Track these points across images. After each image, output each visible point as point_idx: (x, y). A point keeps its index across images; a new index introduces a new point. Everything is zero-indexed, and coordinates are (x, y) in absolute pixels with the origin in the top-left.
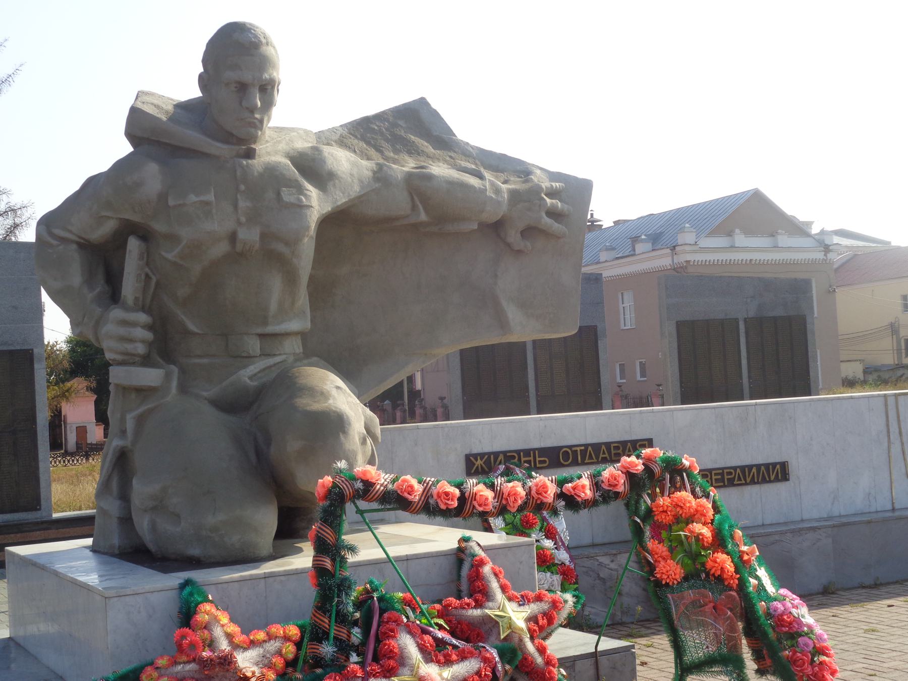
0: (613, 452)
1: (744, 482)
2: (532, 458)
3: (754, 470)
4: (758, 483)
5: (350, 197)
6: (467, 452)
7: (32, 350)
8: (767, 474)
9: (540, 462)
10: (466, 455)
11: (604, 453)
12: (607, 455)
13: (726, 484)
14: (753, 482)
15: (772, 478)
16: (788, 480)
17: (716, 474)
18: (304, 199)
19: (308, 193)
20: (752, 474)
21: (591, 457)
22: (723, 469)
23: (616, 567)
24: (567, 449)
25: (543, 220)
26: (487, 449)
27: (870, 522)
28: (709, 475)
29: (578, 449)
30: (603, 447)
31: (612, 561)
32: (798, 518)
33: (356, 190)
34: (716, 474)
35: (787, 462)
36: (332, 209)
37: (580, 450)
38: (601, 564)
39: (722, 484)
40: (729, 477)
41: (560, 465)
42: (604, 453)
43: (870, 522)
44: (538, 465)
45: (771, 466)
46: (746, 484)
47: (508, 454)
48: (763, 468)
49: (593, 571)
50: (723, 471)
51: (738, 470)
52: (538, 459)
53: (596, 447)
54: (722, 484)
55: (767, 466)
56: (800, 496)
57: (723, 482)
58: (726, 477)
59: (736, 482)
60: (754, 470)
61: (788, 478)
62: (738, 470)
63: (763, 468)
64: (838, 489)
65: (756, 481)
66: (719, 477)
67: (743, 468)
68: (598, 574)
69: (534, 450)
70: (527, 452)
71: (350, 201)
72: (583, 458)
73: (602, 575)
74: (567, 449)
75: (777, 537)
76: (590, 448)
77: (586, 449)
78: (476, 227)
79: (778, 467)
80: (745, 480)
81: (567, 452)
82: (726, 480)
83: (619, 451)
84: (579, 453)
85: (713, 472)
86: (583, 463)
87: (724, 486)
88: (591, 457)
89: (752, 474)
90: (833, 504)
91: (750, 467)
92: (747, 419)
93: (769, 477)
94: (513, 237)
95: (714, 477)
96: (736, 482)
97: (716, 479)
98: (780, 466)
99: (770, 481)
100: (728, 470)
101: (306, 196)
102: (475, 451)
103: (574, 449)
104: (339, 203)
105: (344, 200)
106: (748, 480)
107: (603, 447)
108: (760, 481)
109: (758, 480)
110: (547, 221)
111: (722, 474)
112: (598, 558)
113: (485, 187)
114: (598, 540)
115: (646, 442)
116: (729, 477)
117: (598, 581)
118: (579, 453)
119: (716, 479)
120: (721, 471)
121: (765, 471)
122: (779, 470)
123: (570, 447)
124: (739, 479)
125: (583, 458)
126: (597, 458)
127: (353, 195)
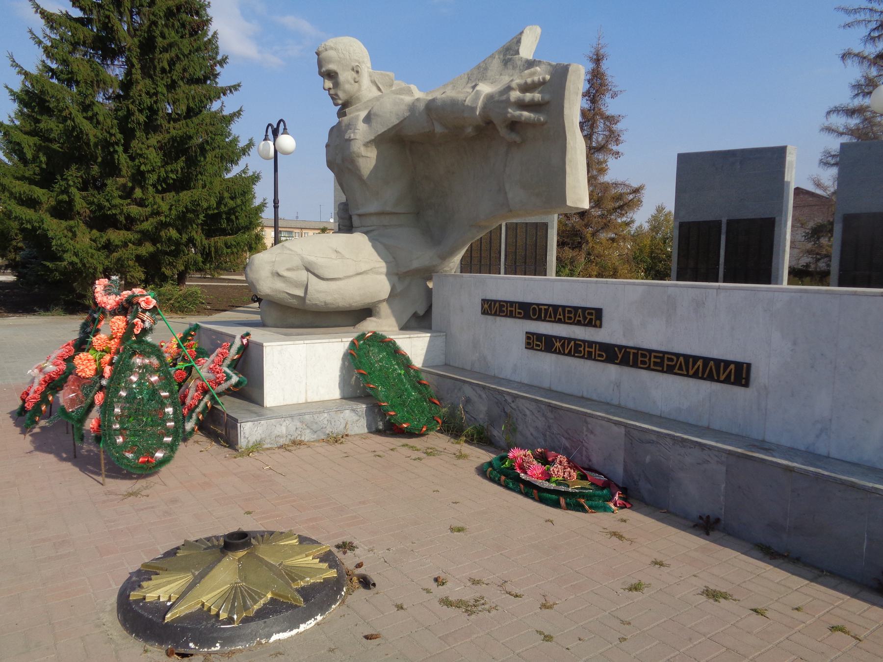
0: (567, 315)
1: (686, 373)
2: (514, 309)
3: (700, 363)
4: (702, 378)
5: (388, 128)
6: (484, 298)
7: (775, 218)
8: (716, 374)
9: (520, 313)
10: (482, 300)
11: (560, 315)
12: (562, 317)
13: (665, 370)
14: (695, 376)
15: (722, 378)
16: (746, 385)
17: (655, 357)
18: (352, 135)
19: (356, 131)
20: (696, 367)
21: (550, 317)
22: (664, 353)
23: (515, 407)
24: (536, 307)
25: (509, 115)
26: (494, 298)
27: (791, 471)
28: (648, 355)
29: (543, 307)
30: (560, 309)
31: (513, 402)
32: (760, 438)
33: (395, 121)
34: (655, 357)
35: (749, 365)
36: (376, 138)
37: (545, 309)
38: (506, 400)
39: (661, 369)
40: (670, 363)
41: (530, 318)
42: (560, 315)
43: (791, 471)
44: (517, 315)
45: (722, 364)
46: (687, 375)
47: (501, 303)
48: (712, 363)
49: (501, 404)
50: (664, 357)
51: (681, 359)
52: (517, 310)
53: (556, 307)
54: (661, 369)
55: (718, 362)
56: (766, 410)
57: (663, 366)
58: (666, 362)
59: (676, 371)
60: (700, 363)
61: (743, 381)
62: (681, 359)
63: (712, 363)
64: (830, 420)
65: (700, 375)
66: (659, 360)
67: (687, 357)
68: (504, 410)
69: (516, 303)
70: (512, 303)
71: (389, 130)
72: (545, 317)
73: (506, 410)
74: (536, 307)
75: (654, 438)
76: (551, 309)
77: (549, 308)
78: (469, 130)
79: (732, 366)
80: (687, 371)
81: (534, 309)
82: (665, 366)
83: (571, 315)
84: (543, 311)
85: (653, 354)
86: (545, 320)
87: (662, 371)
88: (550, 317)
89: (696, 367)
90: (818, 436)
91: (696, 358)
92: (704, 303)
93: (718, 376)
94: (503, 132)
95: (653, 359)
96: (675, 371)
97: (654, 362)
98: (735, 367)
99: (718, 381)
100: (670, 356)
101: (354, 133)
102: (488, 298)
103: (541, 307)
104: (379, 133)
105: (383, 131)
106: (691, 372)
107: (560, 309)
108: (705, 377)
109: (703, 373)
110: (513, 113)
111: (662, 359)
112: (504, 395)
113: (466, 98)
114: (554, 388)
115: (593, 311)
116: (670, 363)
117: (503, 413)
118: (543, 311)
119: (654, 362)
120: (661, 355)
121: (713, 367)
122: (733, 371)
123: (538, 305)
124: (680, 368)
125: (545, 317)
126: (555, 317)
127: (391, 126)
